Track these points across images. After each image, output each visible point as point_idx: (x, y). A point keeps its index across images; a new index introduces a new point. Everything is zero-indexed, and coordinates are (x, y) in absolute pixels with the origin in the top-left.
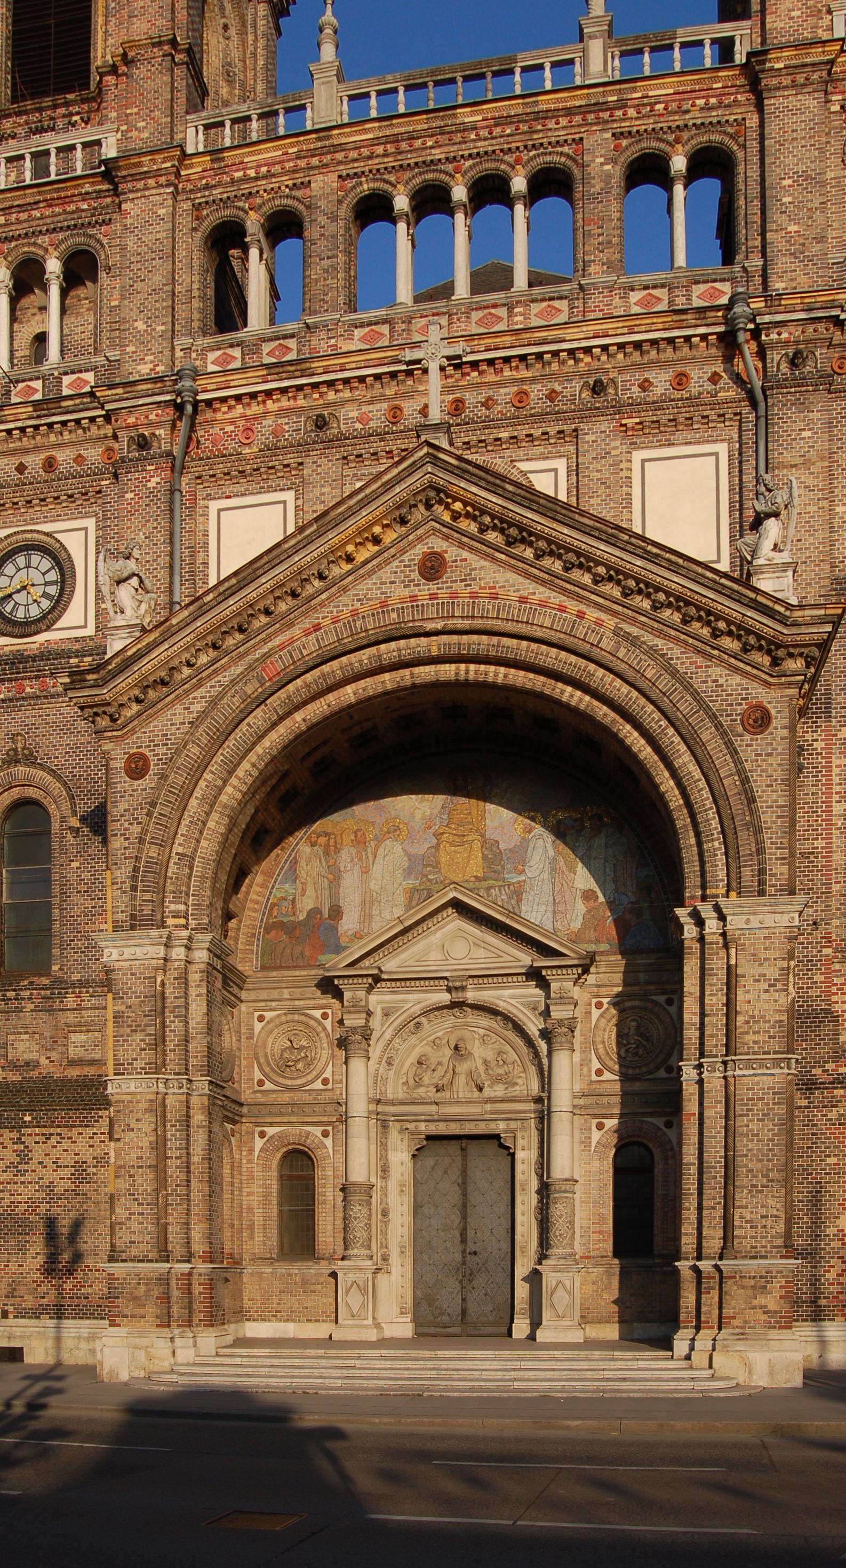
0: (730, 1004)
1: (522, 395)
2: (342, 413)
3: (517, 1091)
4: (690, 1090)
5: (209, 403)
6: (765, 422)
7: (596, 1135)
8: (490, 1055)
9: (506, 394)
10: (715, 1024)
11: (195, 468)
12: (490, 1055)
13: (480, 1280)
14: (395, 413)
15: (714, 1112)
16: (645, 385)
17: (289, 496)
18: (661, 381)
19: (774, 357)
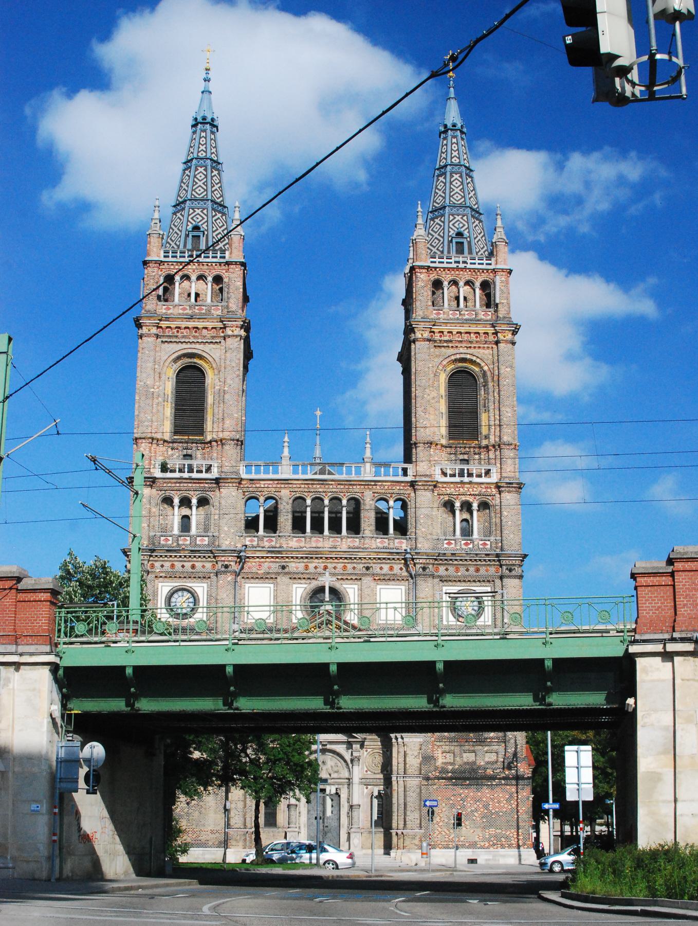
0: (405, 761)
1: (345, 567)
2: (289, 564)
3: (342, 776)
4: (394, 783)
5: (248, 557)
6: (415, 584)
7: (366, 790)
8: (333, 764)
9: (340, 566)
10: (401, 766)
11: (242, 575)
12: (333, 764)
13: (329, 835)
14: (307, 567)
15: (401, 789)
16: (381, 568)
17: (272, 586)
18: (386, 568)
19: (418, 566)
